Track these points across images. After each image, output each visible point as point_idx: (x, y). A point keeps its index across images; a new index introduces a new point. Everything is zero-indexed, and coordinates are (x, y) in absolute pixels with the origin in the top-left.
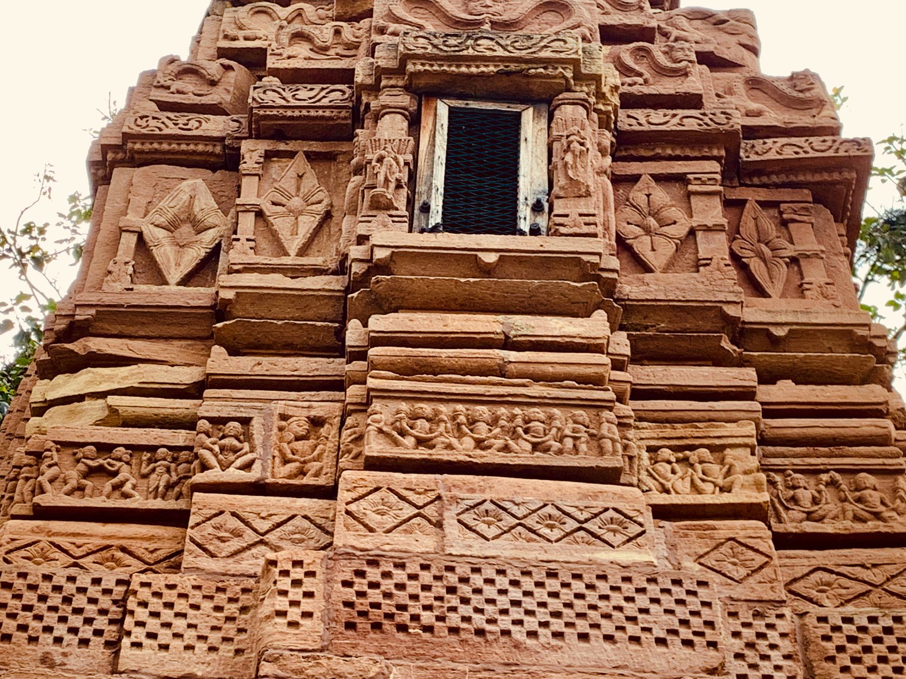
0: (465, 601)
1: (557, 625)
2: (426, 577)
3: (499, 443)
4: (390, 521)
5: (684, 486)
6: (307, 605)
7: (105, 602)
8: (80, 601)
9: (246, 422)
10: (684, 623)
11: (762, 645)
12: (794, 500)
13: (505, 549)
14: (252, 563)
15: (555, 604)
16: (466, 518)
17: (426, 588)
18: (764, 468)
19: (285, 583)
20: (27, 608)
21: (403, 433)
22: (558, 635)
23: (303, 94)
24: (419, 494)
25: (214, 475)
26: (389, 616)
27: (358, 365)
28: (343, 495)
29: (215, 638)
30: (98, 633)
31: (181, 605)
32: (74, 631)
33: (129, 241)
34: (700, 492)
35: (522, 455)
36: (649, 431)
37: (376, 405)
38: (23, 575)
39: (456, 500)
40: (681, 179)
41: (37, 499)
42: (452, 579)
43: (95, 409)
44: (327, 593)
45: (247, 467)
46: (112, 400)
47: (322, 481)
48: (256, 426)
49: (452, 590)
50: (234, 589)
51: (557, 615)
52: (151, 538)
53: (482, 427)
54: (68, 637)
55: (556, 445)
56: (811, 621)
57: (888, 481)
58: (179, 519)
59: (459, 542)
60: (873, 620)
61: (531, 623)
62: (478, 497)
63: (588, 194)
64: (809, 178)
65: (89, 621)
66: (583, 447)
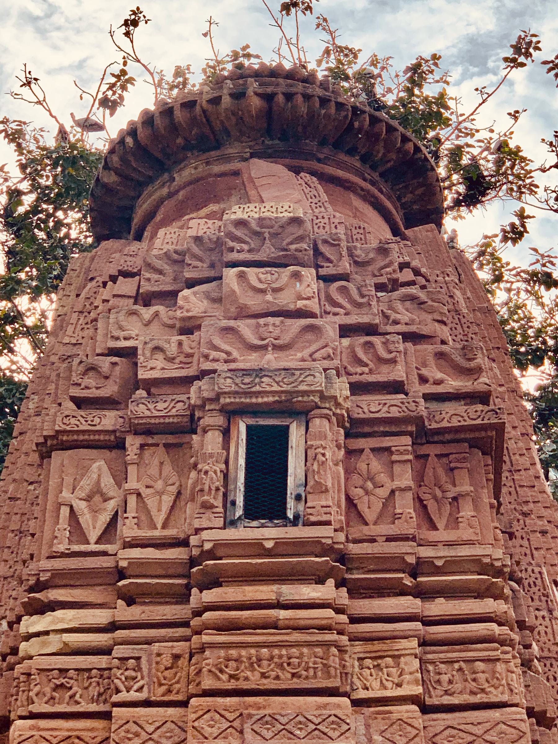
3: (273, 674)
4: (215, 731)
5: (376, 684)
9: (138, 659)
12: (439, 682)
16: (255, 727)
23: (161, 406)
24: (231, 712)
25: (123, 696)
33: (65, 511)
34: (386, 688)
36: (359, 648)
37: (207, 653)
40: (388, 449)
41: (31, 708)
48: (144, 661)
52: (92, 730)
53: (265, 663)
55: (304, 673)
57: (490, 666)
58: (107, 716)
62: (262, 712)
63: (327, 491)
64: (467, 436)
66: (319, 674)
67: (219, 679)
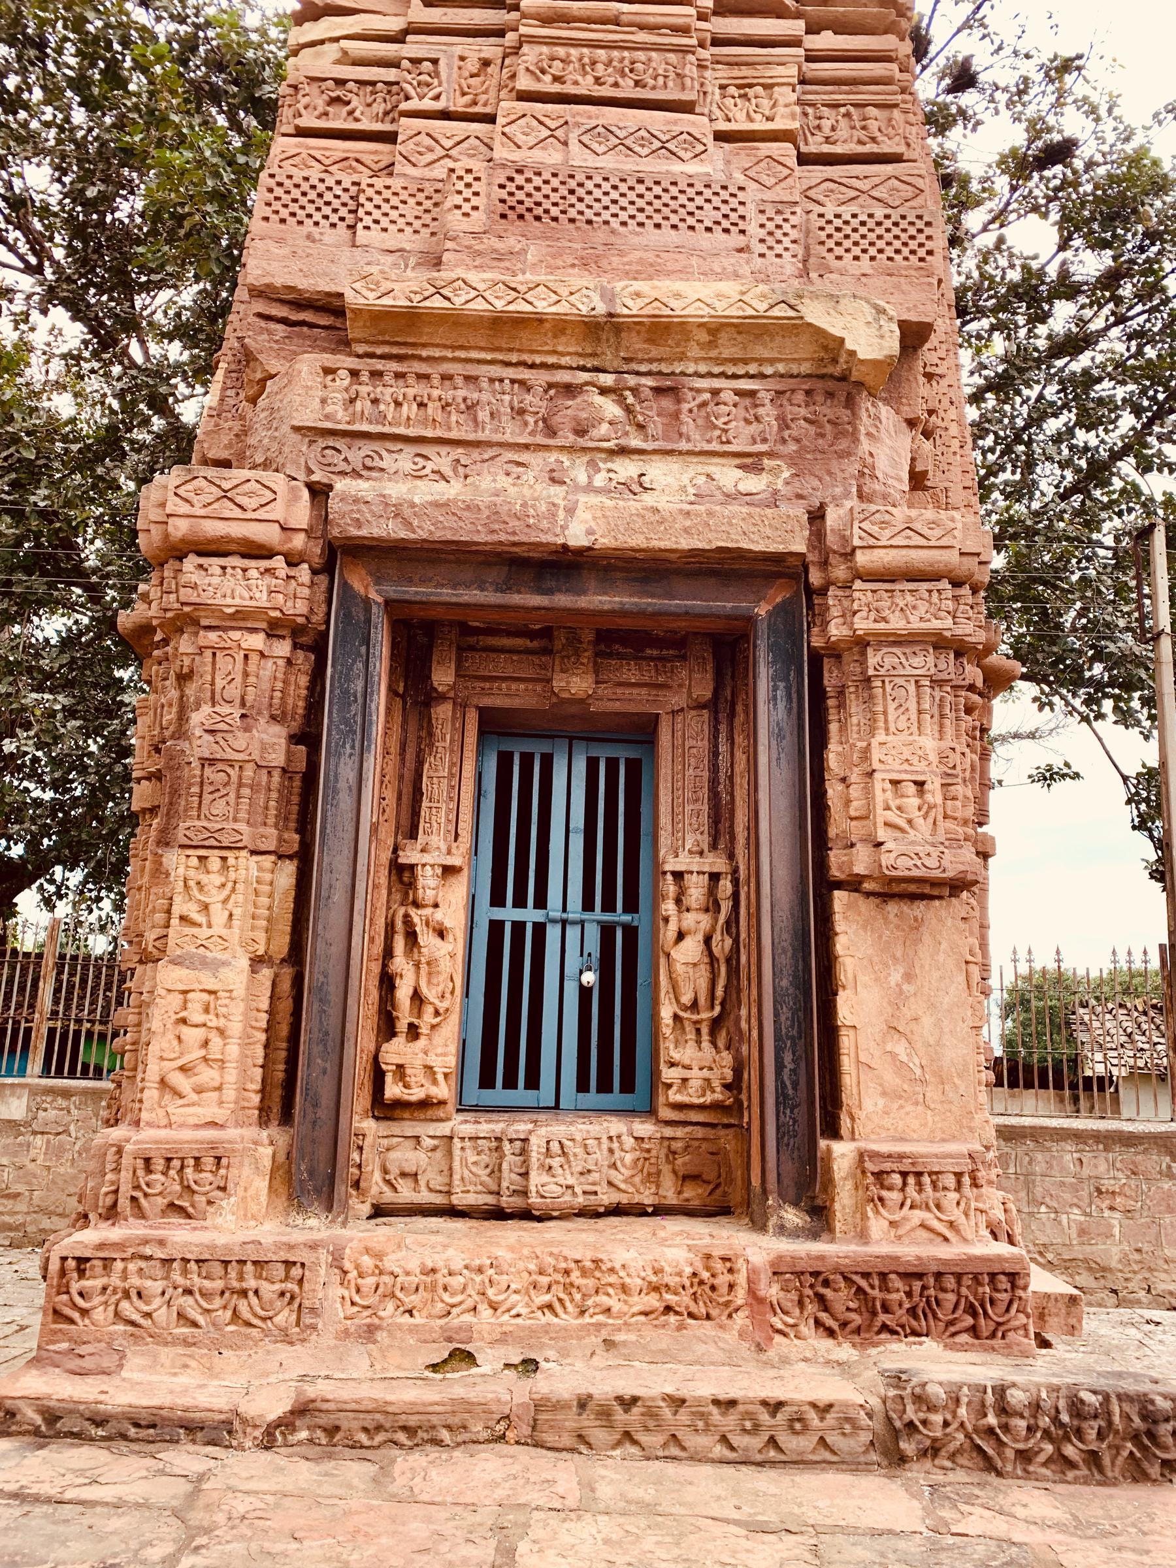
0: (581, 200)
1: (641, 217)
2: (555, 182)
3: (611, 80)
4: (532, 141)
5: (741, 116)
6: (475, 201)
7: (345, 198)
8: (328, 196)
9: (435, 62)
10: (726, 216)
11: (778, 234)
12: (819, 127)
13: (609, 162)
14: (439, 171)
15: (640, 203)
16: (585, 139)
17: (555, 190)
18: (799, 102)
19: (460, 185)
20: (295, 201)
21: (543, 72)
22: (641, 224)
26: (529, 210)
27: (515, 15)
28: (500, 120)
29: (417, 224)
30: (342, 219)
31: (395, 201)
32: (326, 217)
34: (751, 120)
35: (628, 91)
36: (723, 72)
37: (526, 49)
38: (290, 177)
39: (578, 125)
41: (298, 121)
42: (572, 184)
43: (332, 50)
44: (489, 194)
45: (437, 98)
46: (344, 44)
47: (488, 110)
48: (442, 64)
49: (572, 192)
50: (429, 189)
51: (641, 210)
52: (375, 152)
53: (600, 67)
54: (323, 222)
55: (651, 82)
56: (813, 216)
59: (579, 157)
60: (854, 216)
61: (624, 216)
62: (593, 123)
65: (335, 211)
66: (670, 84)
67: (539, 80)
